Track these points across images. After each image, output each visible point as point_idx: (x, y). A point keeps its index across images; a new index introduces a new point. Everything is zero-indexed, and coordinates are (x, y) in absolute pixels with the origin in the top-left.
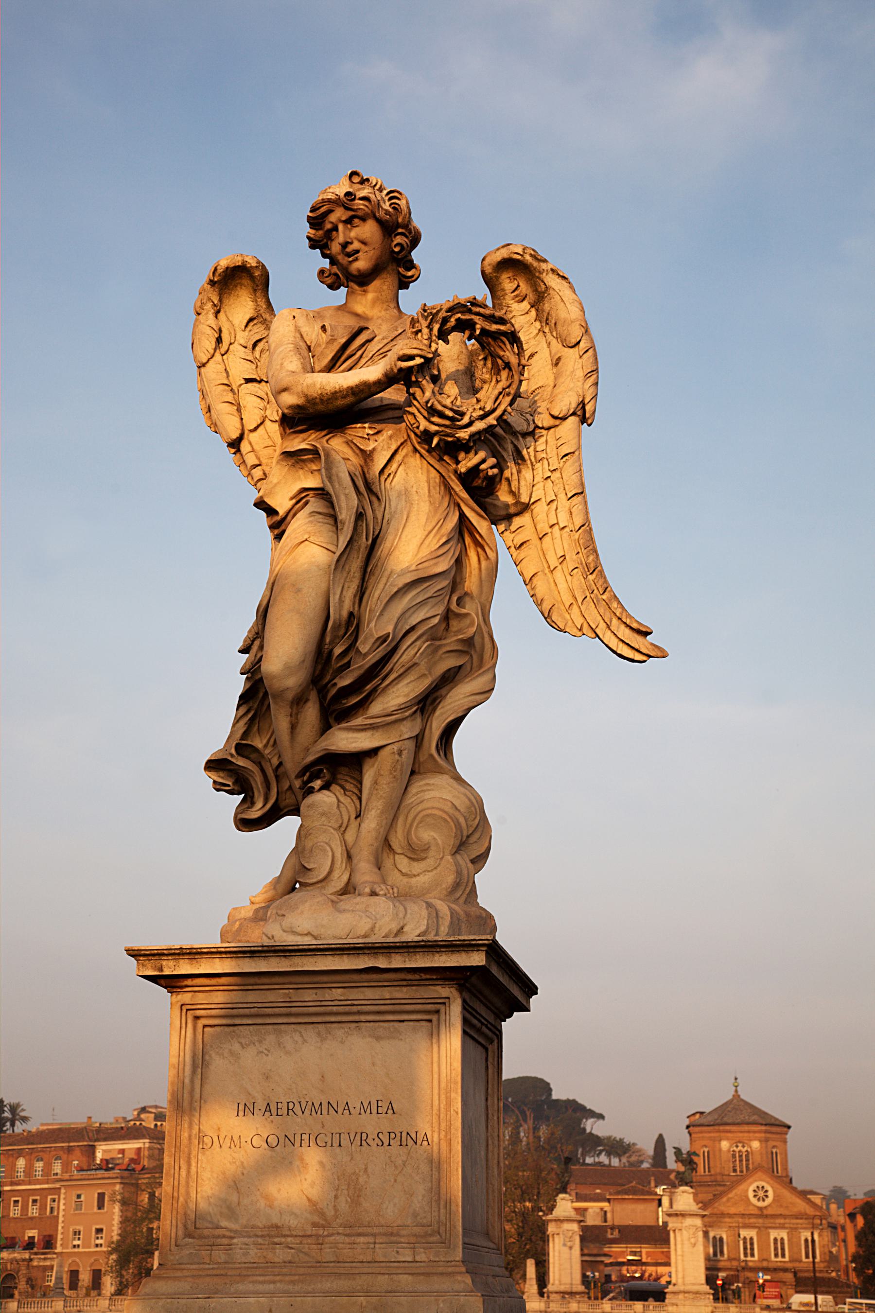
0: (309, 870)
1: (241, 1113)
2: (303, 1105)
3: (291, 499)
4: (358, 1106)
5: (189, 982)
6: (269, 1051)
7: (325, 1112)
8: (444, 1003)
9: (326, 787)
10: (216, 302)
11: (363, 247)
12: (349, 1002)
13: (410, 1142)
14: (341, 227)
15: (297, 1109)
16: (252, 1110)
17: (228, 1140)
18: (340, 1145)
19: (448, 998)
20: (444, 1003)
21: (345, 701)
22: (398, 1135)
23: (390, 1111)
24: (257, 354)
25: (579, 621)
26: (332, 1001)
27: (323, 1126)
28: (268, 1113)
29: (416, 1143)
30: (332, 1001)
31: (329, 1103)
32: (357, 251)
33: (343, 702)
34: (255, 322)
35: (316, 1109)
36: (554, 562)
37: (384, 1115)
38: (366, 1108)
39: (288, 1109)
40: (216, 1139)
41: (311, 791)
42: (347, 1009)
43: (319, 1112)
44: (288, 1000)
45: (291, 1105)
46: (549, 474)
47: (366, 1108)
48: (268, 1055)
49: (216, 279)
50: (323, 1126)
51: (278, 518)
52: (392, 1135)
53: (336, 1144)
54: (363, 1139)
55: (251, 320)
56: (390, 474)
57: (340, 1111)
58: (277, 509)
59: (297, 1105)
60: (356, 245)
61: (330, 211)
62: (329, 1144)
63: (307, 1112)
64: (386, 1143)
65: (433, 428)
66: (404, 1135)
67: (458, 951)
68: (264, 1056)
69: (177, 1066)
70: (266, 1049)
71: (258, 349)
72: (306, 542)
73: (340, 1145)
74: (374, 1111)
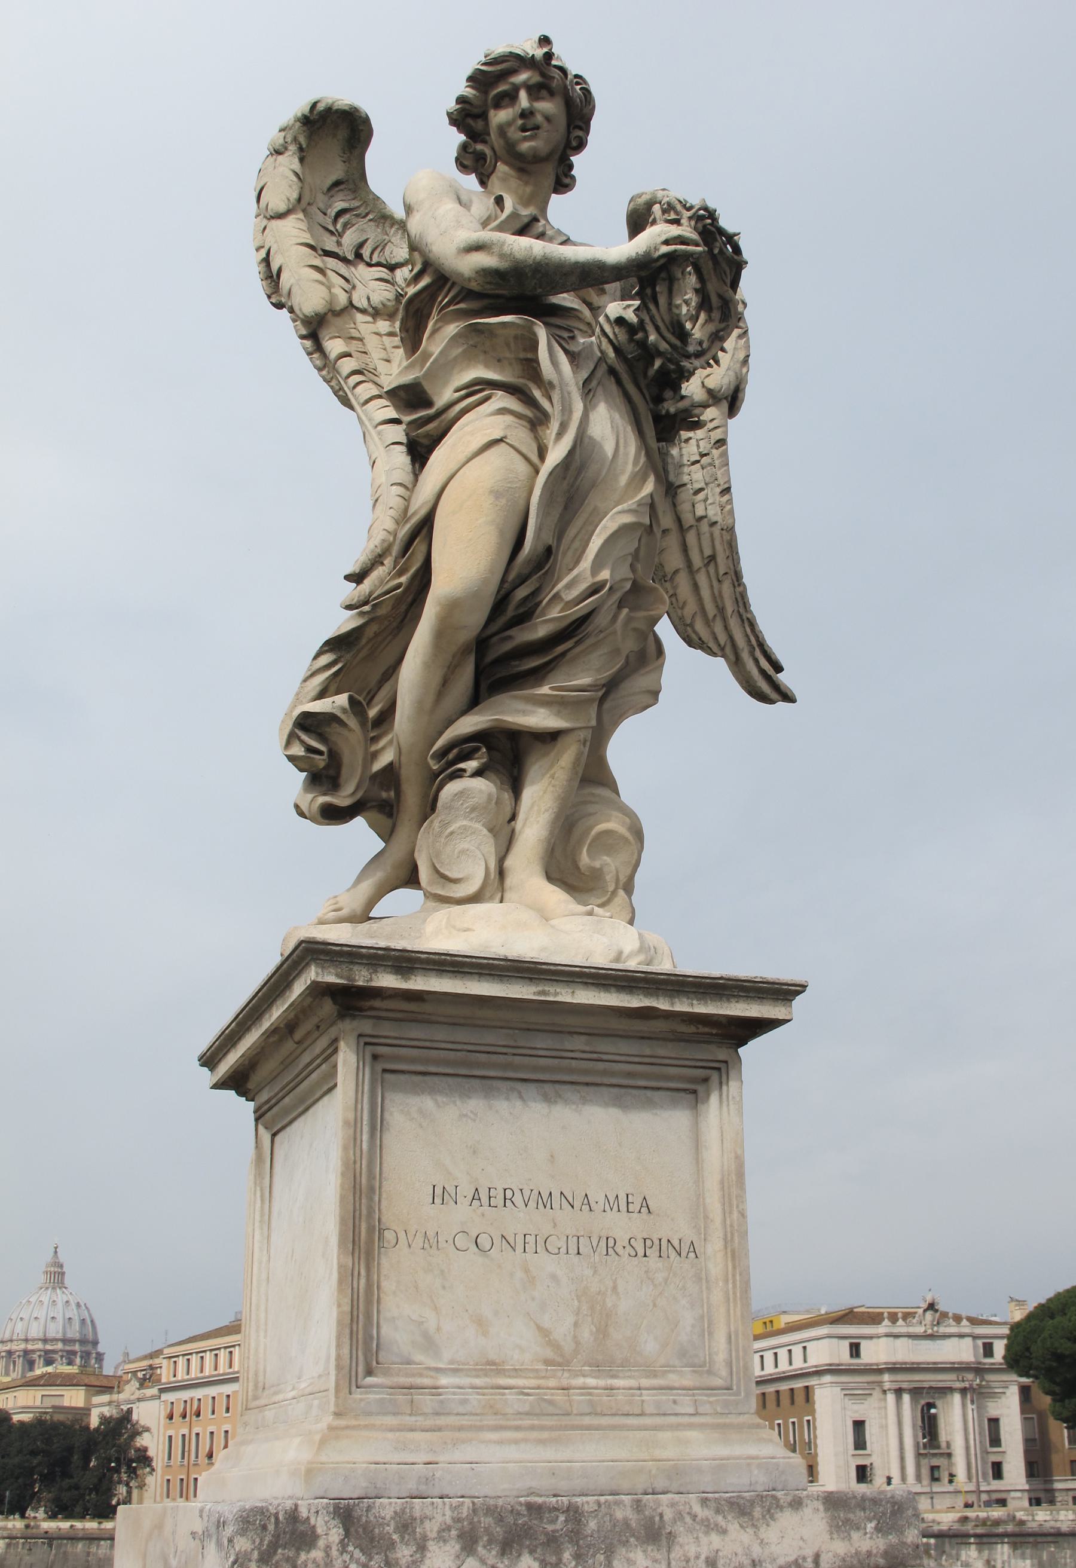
0: (455, 881)
1: (438, 1200)
2: (527, 1193)
3: (457, 391)
4: (602, 1199)
5: (377, 1003)
6: (476, 1115)
7: (556, 1205)
8: (719, 1069)
9: (478, 773)
10: (304, 146)
11: (545, 125)
12: (595, 1056)
13: (673, 1254)
14: (523, 95)
15: (518, 1199)
16: (453, 1195)
17: (419, 1239)
18: (578, 1253)
19: (726, 1062)
20: (719, 1069)
21: (517, 663)
22: (657, 1242)
23: (644, 1210)
24: (339, 226)
25: (723, 638)
26: (572, 1051)
27: (555, 1225)
28: (476, 1203)
29: (680, 1255)
30: (572, 1051)
31: (561, 1193)
32: (537, 128)
33: (513, 663)
34: (342, 187)
35: (545, 1201)
36: (697, 561)
37: (635, 1215)
38: (612, 1203)
39: (505, 1199)
40: (402, 1235)
41: (459, 774)
42: (591, 1064)
43: (549, 1206)
44: (512, 1043)
45: (509, 1194)
46: (698, 458)
47: (612, 1203)
48: (474, 1120)
49: (312, 118)
50: (555, 1225)
51: (431, 411)
52: (648, 1243)
53: (573, 1250)
54: (610, 1245)
55: (337, 184)
56: (590, 390)
57: (577, 1205)
58: (435, 399)
59: (518, 1193)
60: (539, 118)
61: (513, 72)
62: (563, 1250)
63: (532, 1204)
64: (641, 1253)
65: (664, 346)
66: (664, 1242)
67: (759, 998)
68: (469, 1121)
69: (353, 1123)
70: (472, 1112)
71: (341, 221)
72: (503, 444)
73: (578, 1253)
74: (623, 1208)
